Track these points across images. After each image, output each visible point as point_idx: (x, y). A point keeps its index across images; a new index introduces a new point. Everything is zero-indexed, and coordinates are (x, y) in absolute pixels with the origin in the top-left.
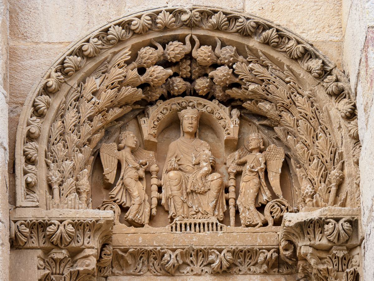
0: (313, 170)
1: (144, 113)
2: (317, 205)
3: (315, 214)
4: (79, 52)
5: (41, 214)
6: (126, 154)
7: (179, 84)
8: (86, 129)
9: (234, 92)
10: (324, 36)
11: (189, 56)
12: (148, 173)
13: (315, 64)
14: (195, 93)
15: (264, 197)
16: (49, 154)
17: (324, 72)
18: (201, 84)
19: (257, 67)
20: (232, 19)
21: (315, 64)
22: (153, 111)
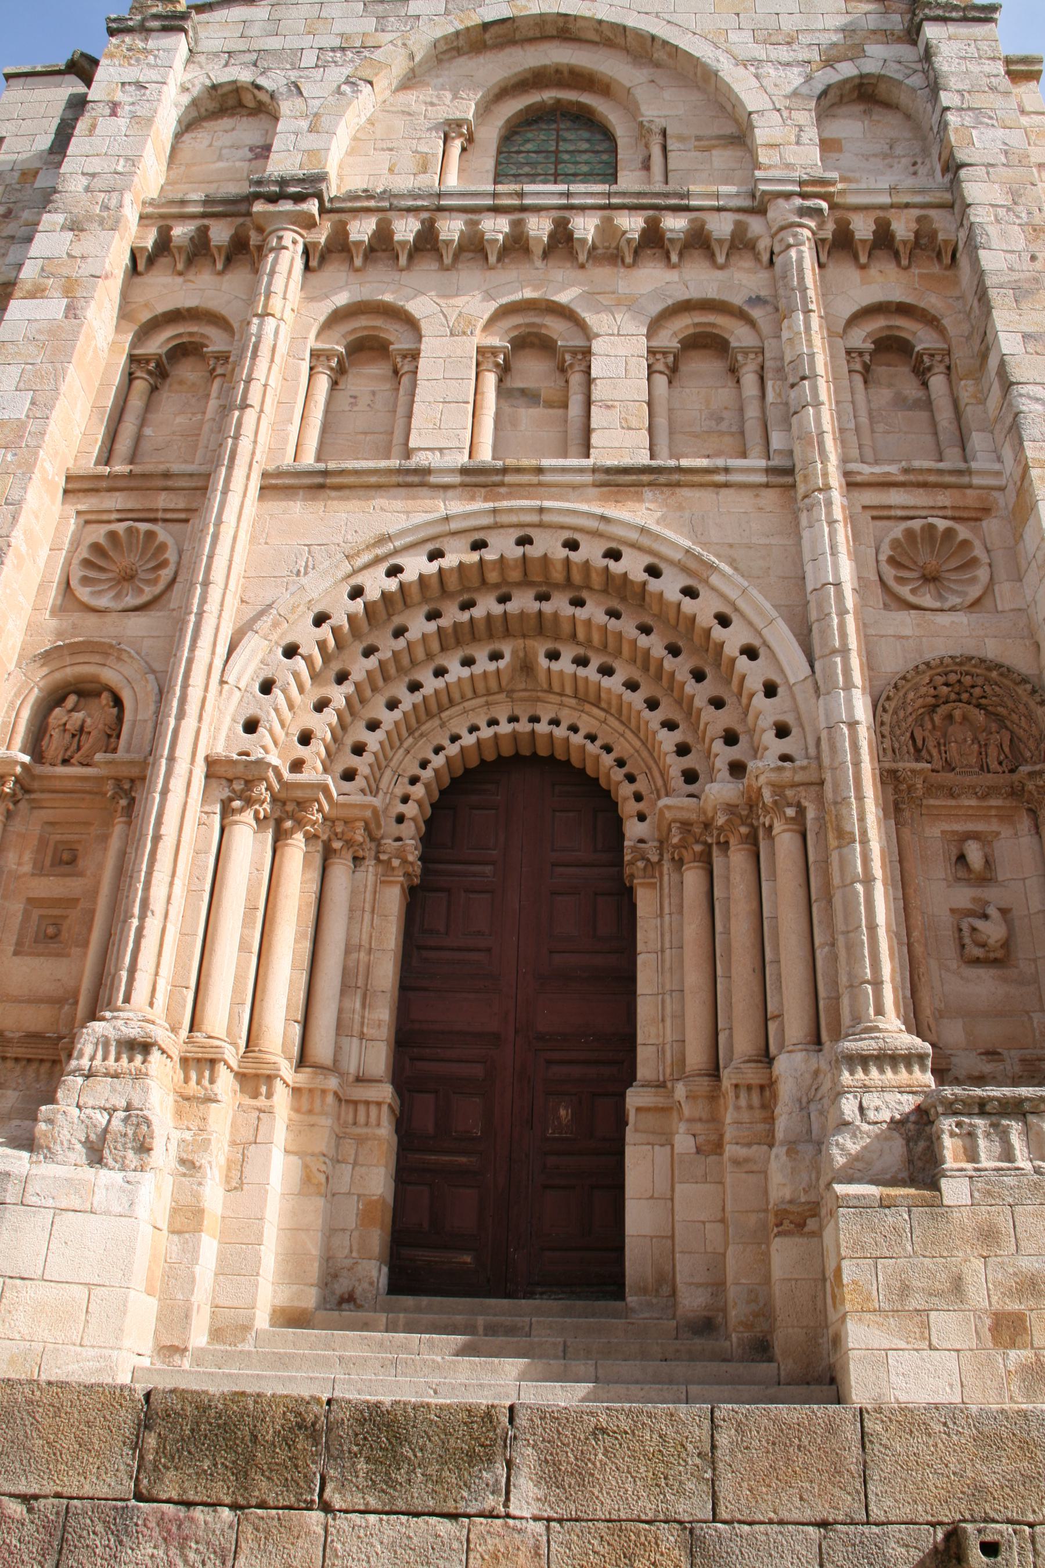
0: (1031, 744)
1: (933, 711)
2: (1035, 763)
3: (1038, 768)
4: (904, 678)
5: (894, 766)
6: (927, 733)
7: (953, 696)
8: (910, 719)
9: (983, 701)
10: (1030, 672)
11: (959, 681)
12: (939, 744)
13: (1029, 687)
14: (960, 701)
15: (1002, 757)
16: (892, 732)
17: (1034, 691)
18: (965, 696)
19: (997, 689)
20: (982, 661)
21: (1029, 687)
22: (940, 710)
